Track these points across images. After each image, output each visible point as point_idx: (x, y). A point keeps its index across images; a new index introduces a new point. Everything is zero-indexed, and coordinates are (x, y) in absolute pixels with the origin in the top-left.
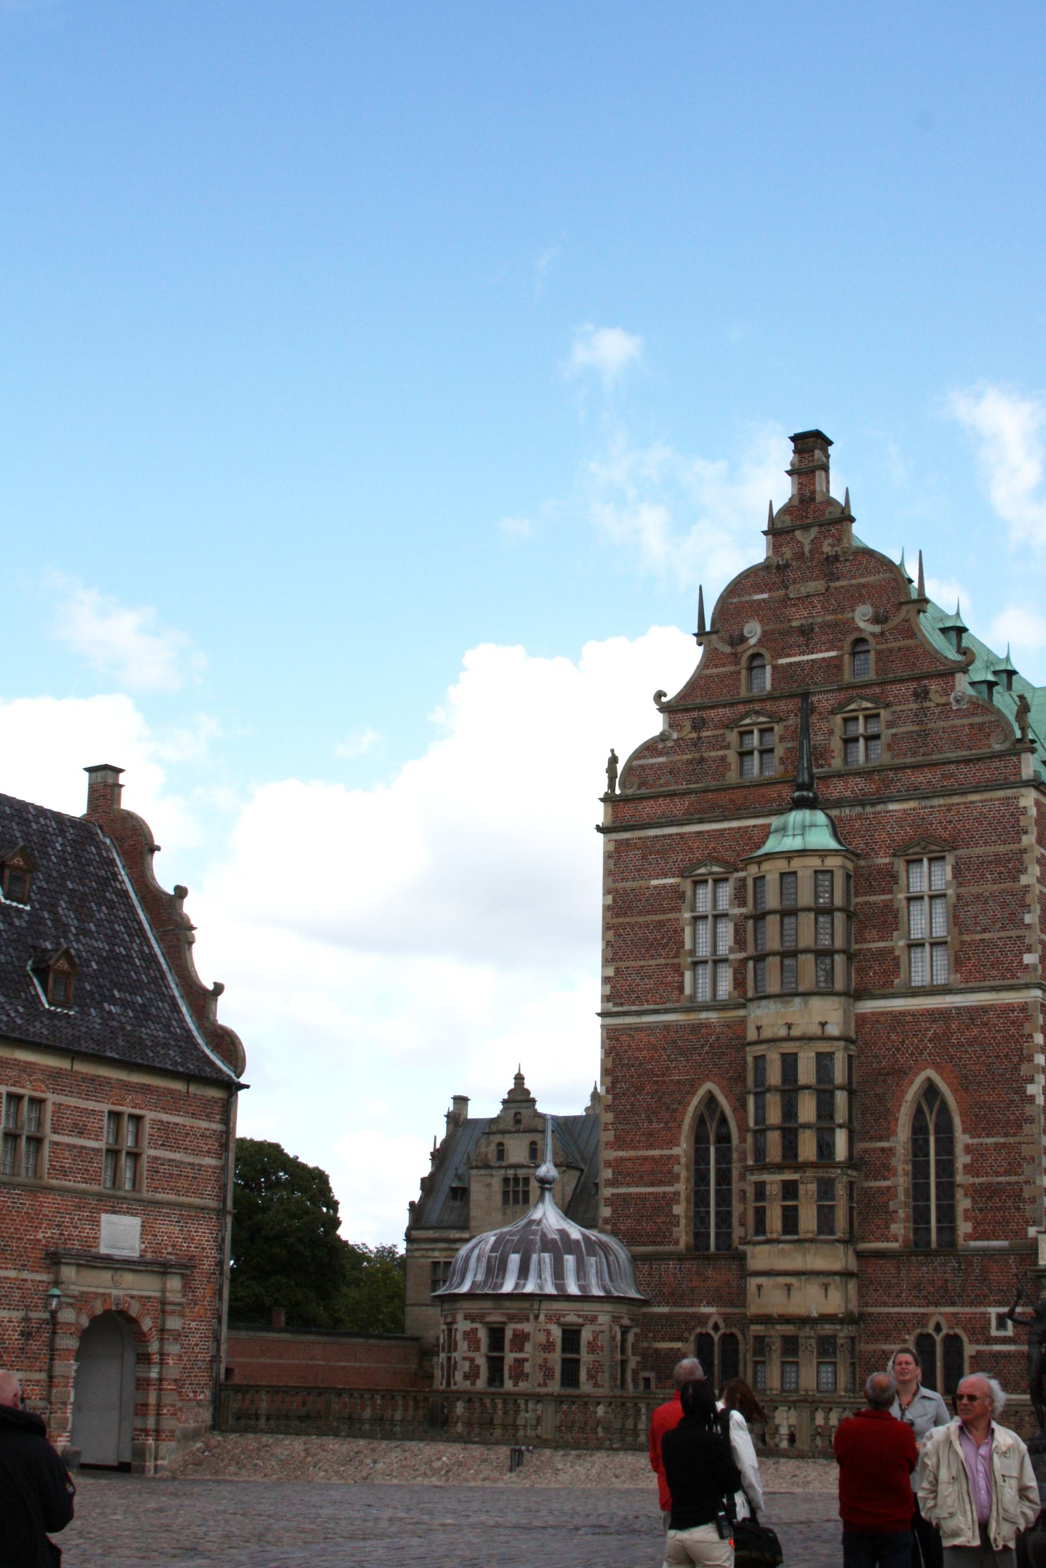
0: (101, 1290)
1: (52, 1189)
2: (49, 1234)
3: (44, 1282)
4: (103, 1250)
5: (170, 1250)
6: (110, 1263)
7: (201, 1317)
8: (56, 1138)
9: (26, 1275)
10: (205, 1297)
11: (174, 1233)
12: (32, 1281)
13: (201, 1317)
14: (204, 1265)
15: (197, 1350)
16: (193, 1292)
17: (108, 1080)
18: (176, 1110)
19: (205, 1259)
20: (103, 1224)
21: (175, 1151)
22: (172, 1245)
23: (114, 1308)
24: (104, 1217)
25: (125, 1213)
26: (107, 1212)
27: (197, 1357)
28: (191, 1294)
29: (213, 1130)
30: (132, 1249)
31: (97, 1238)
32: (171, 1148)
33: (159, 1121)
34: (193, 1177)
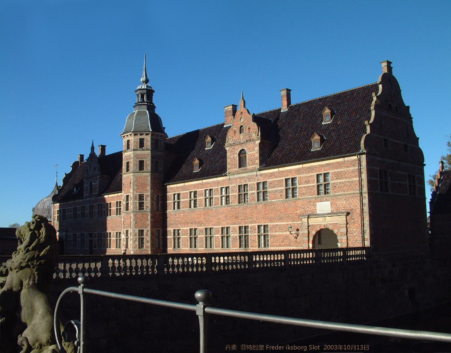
0: (319, 223)
1: (299, 199)
2: (301, 211)
3: (300, 223)
4: (318, 213)
5: (343, 208)
6: (323, 215)
7: (357, 227)
8: (300, 186)
9: (294, 222)
10: (359, 221)
11: (344, 203)
12: (297, 224)
13: (357, 227)
14: (357, 211)
15: (356, 237)
16: (353, 220)
17: (315, 166)
18: (342, 167)
19: (358, 209)
20: (317, 205)
21: (341, 179)
22: (343, 207)
23: (323, 228)
24: (318, 204)
25: (325, 201)
26: (318, 202)
27: (357, 239)
28: (353, 220)
29: (356, 169)
30: (329, 210)
31: (316, 209)
32: (340, 179)
33: (334, 172)
34: (350, 185)
